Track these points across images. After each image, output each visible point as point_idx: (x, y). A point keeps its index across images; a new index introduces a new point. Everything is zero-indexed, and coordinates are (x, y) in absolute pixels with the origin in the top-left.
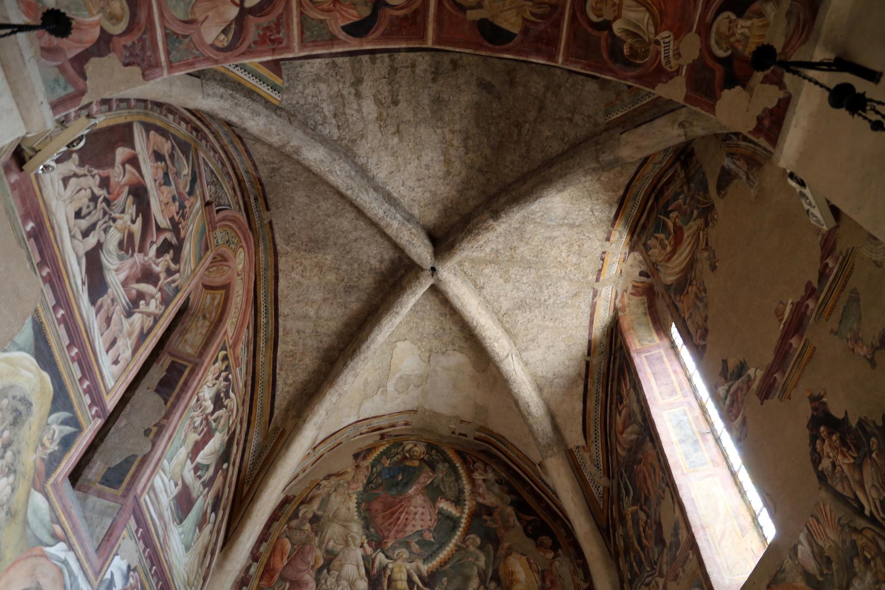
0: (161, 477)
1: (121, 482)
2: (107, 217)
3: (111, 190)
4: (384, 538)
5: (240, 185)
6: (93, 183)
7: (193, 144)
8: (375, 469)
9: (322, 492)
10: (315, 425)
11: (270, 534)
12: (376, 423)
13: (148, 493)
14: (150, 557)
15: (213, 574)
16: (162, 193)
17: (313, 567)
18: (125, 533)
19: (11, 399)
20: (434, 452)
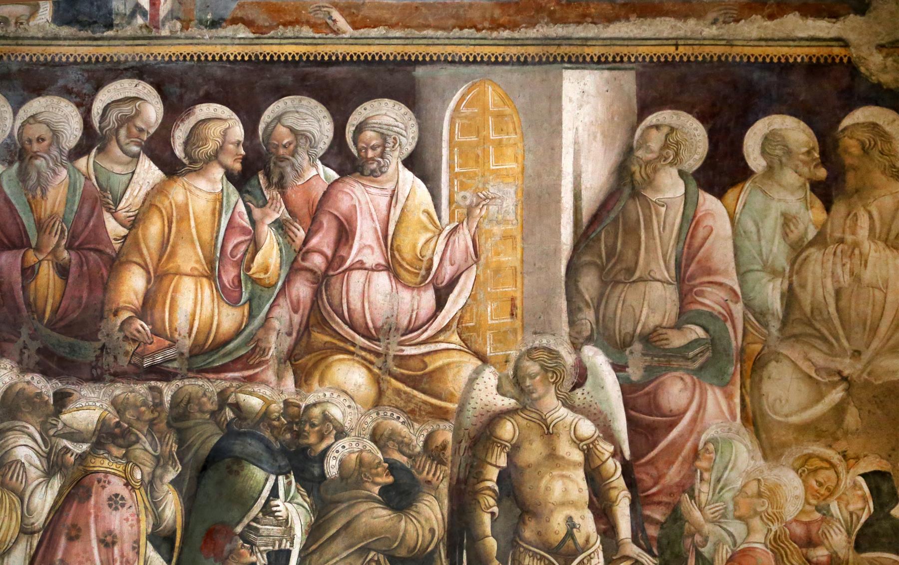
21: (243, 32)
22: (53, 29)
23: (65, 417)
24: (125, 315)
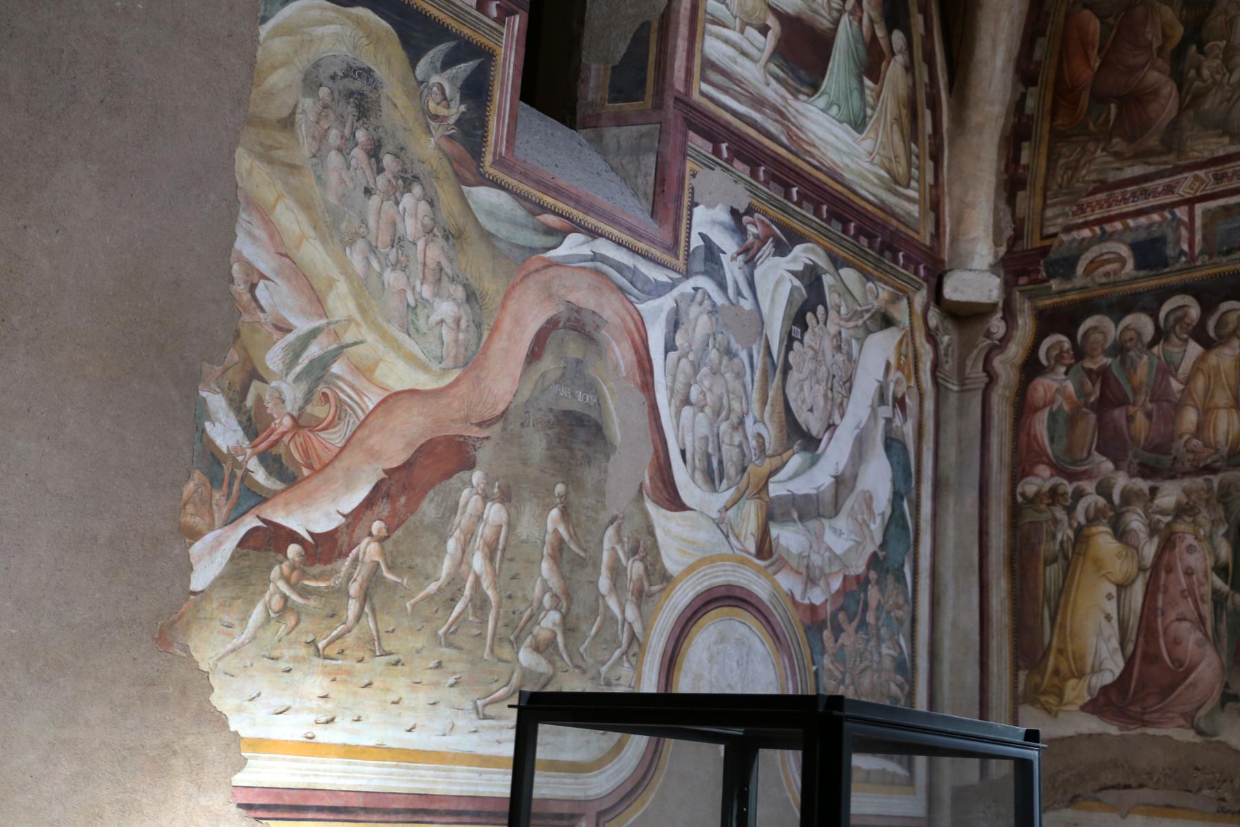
0: (718, 37)
1: (642, 83)
13: (704, 79)
14: (772, 178)
15: (951, 142)
17: (1161, 49)
18: (690, 165)
19: (330, 83)
22: (1135, 273)
23: (1157, 502)
24: (1186, 437)
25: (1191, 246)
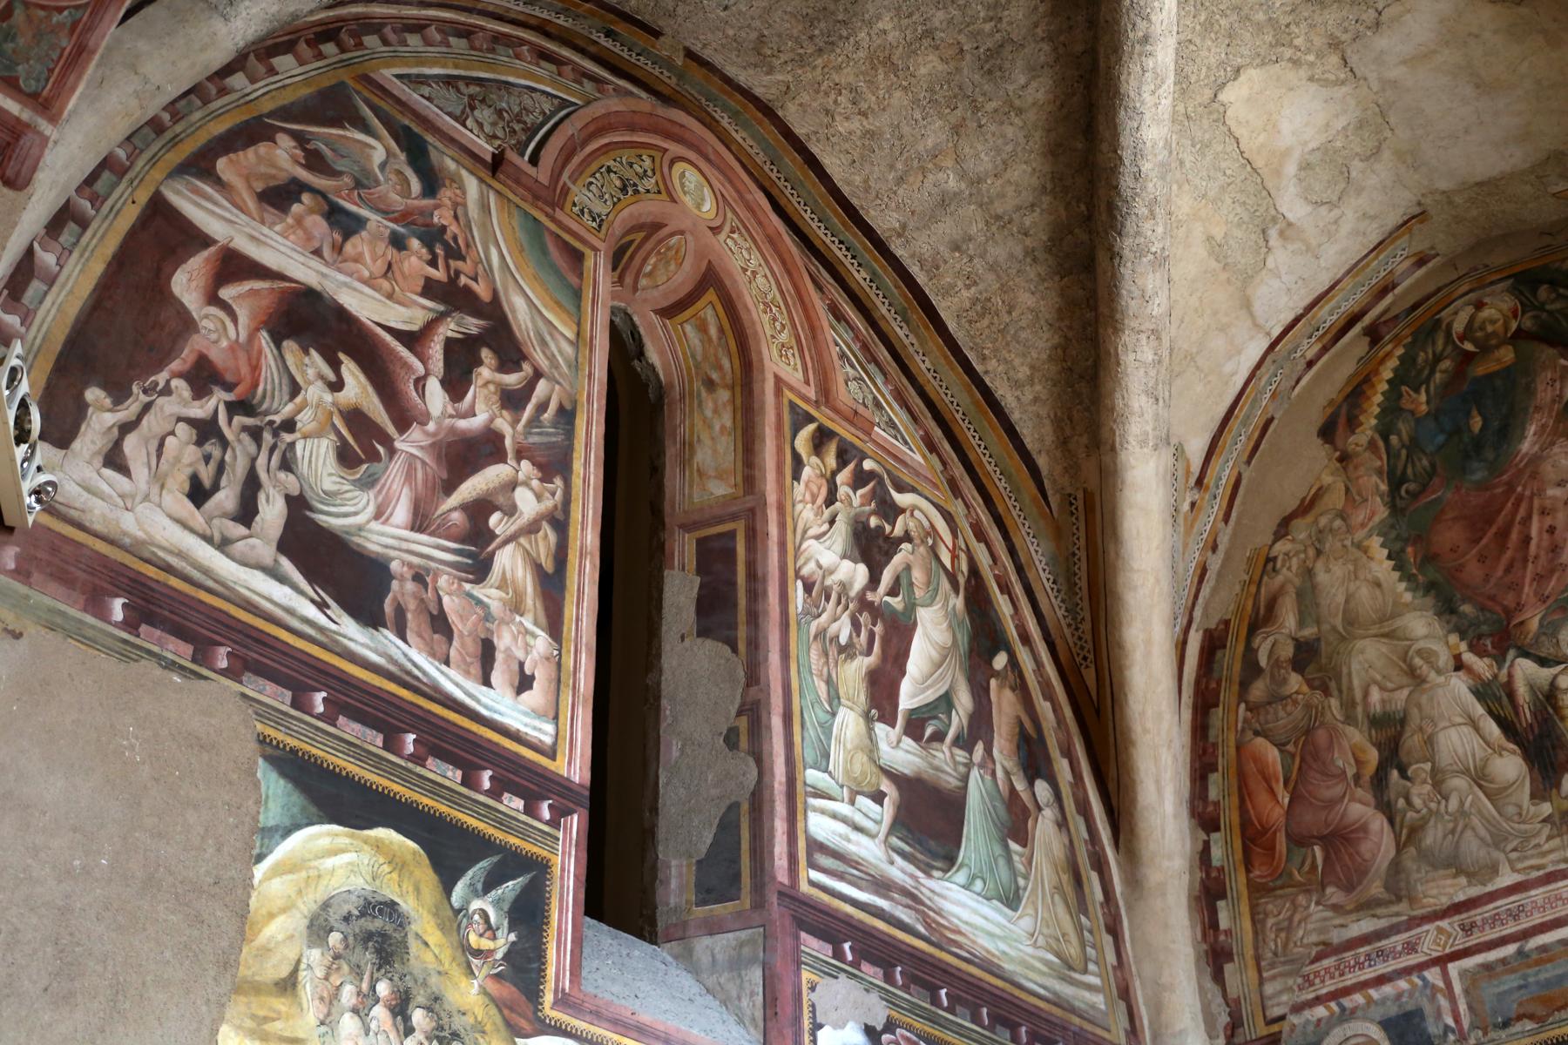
0: (823, 812)
1: (737, 877)
2: (267, 437)
3: (229, 378)
4: (1509, 614)
5: (548, 35)
6: (181, 401)
7: (345, 76)
8: (1394, 439)
9: (1288, 574)
10: (1143, 443)
11: (1215, 745)
12: (1328, 316)
13: (812, 865)
14: (912, 980)
15: (1129, 909)
16: (357, 259)
17: (1357, 778)
18: (806, 975)
19: (343, 926)
20: (1543, 292)
21: (1529, 1025)
25: (1457, 1019)
